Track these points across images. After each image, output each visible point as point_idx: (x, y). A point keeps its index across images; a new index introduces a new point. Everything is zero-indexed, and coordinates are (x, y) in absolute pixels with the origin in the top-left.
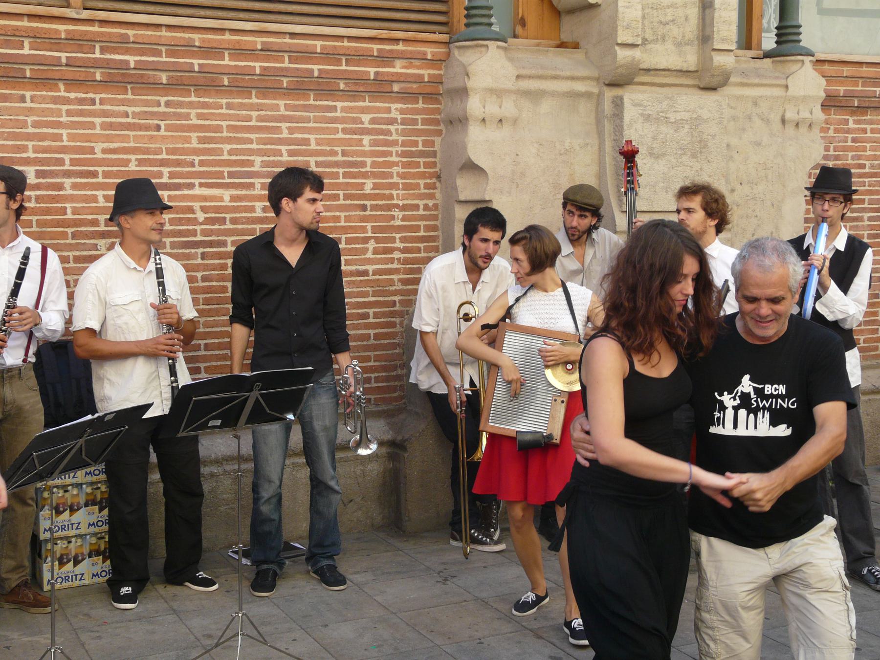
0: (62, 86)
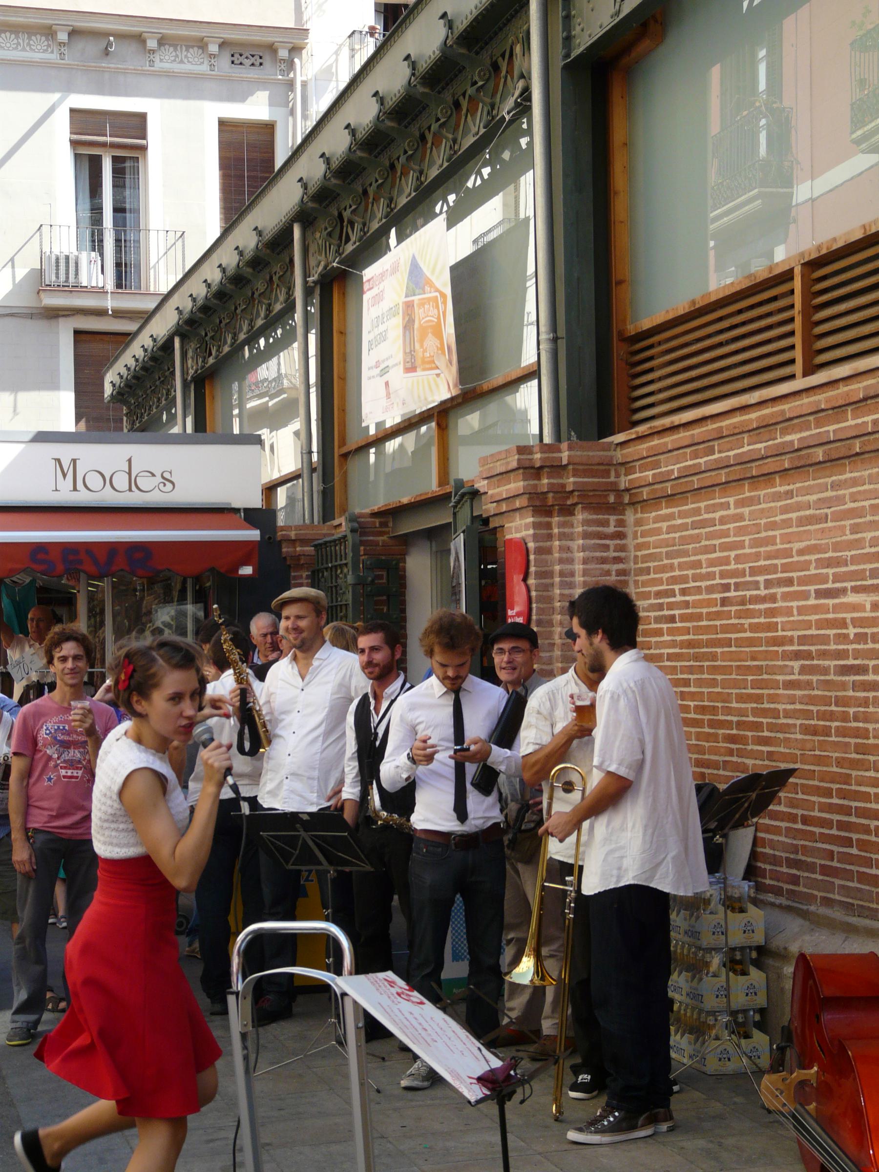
0: (778, 480)
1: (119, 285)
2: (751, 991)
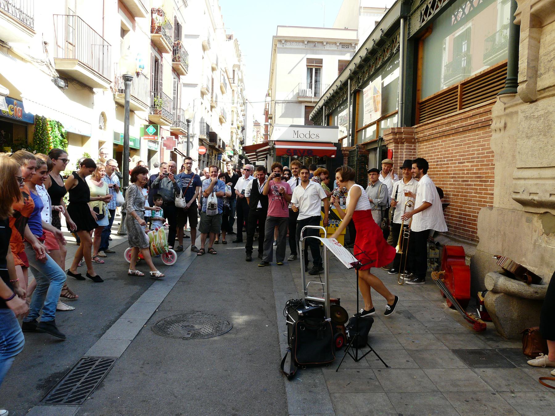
1: (315, 96)
2: (435, 254)
